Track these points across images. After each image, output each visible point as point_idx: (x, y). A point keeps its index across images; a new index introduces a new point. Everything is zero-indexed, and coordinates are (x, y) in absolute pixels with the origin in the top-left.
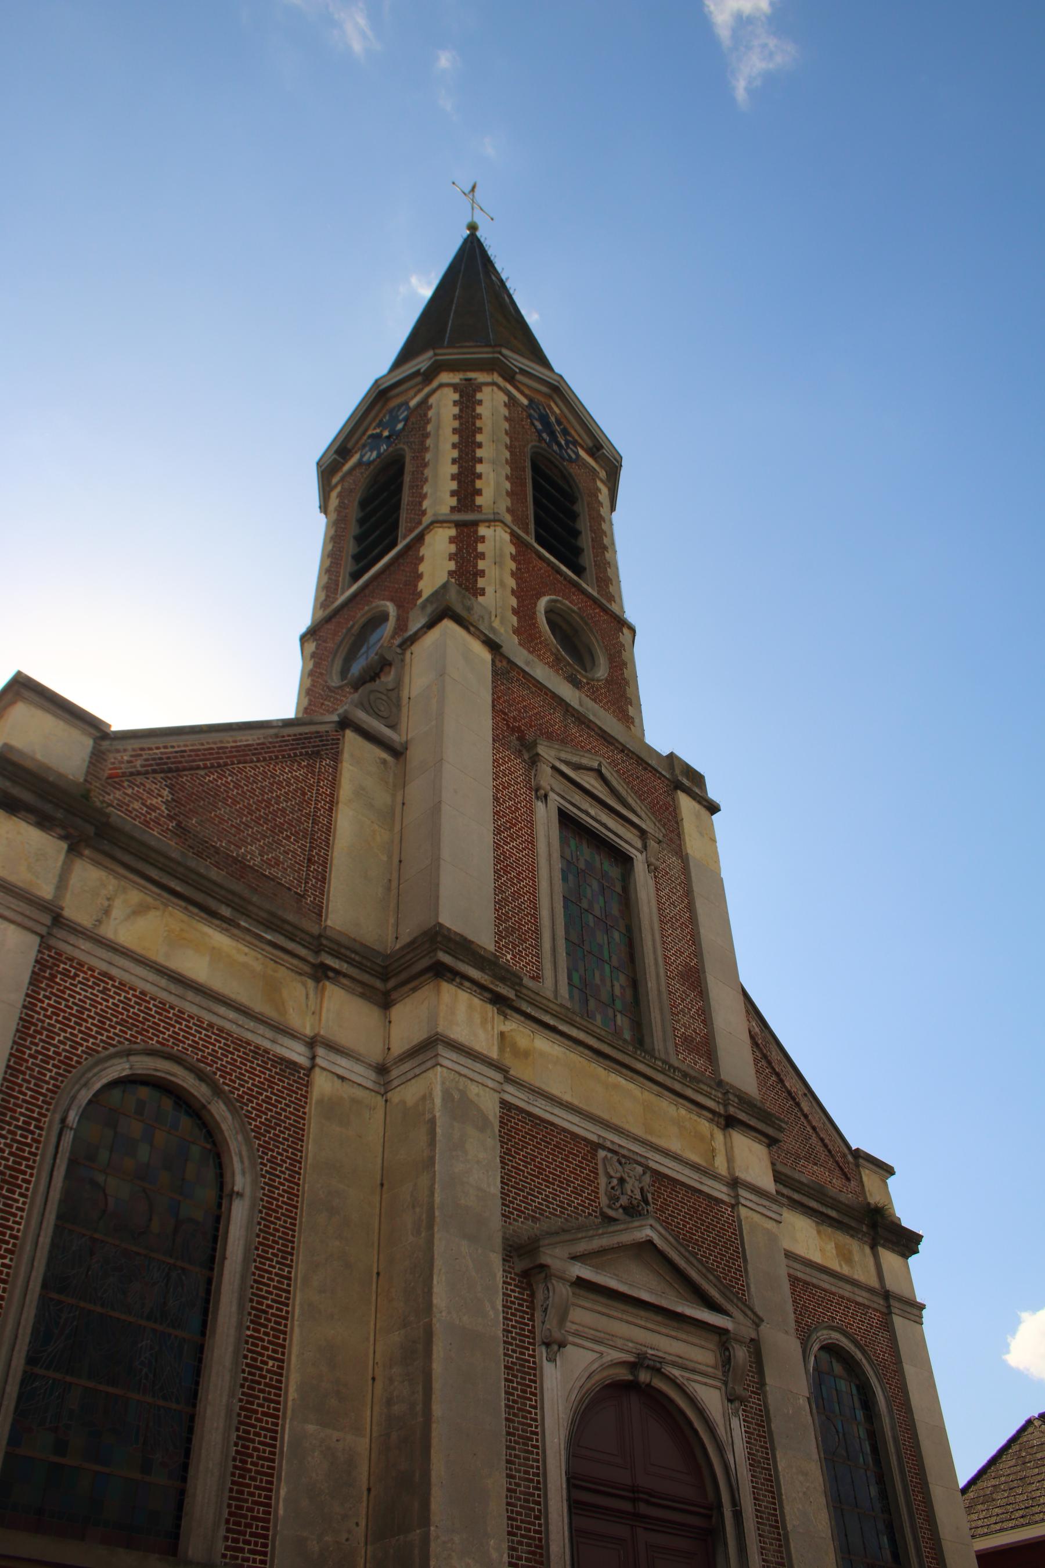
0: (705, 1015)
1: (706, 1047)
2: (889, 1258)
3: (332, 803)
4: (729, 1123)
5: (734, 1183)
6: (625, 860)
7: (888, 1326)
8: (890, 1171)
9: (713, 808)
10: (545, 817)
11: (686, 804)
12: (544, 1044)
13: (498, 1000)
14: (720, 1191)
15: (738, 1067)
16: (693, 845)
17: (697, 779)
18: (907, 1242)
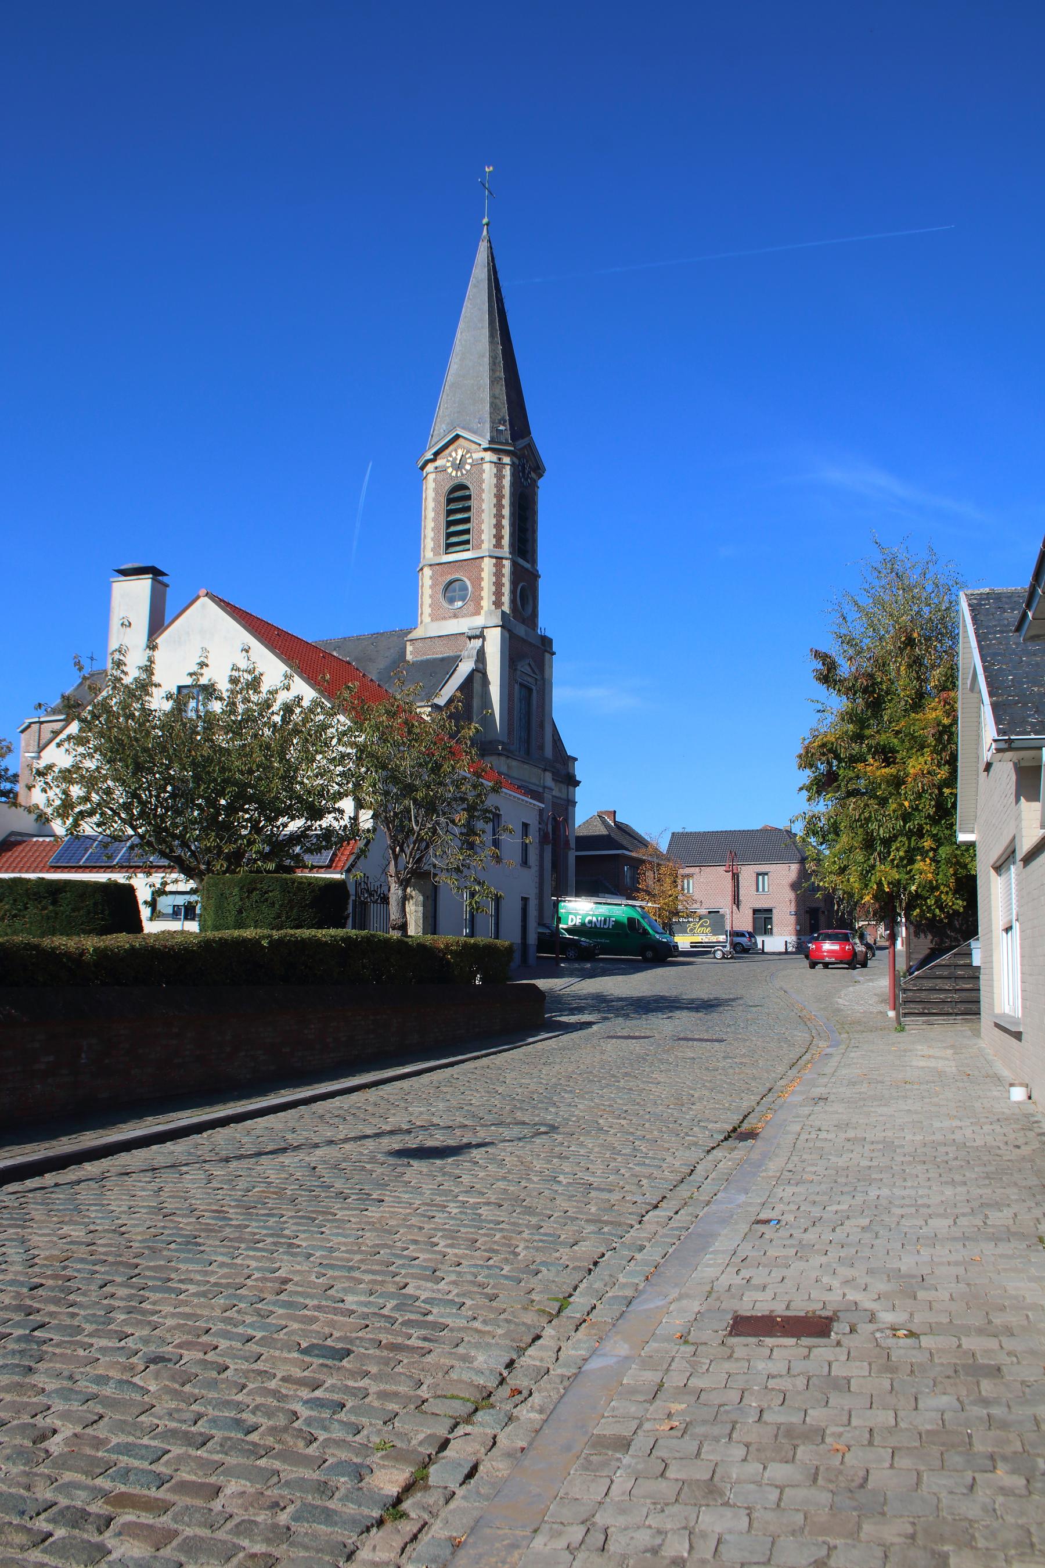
0: (543, 738)
1: (541, 747)
2: (571, 788)
3: (472, 697)
4: (545, 770)
5: (544, 787)
6: (530, 690)
7: (567, 809)
8: (576, 759)
9: (554, 654)
10: (517, 687)
11: (547, 655)
12: (514, 763)
13: (508, 757)
14: (540, 790)
15: (549, 752)
16: (546, 676)
17: (550, 641)
18: (578, 783)
